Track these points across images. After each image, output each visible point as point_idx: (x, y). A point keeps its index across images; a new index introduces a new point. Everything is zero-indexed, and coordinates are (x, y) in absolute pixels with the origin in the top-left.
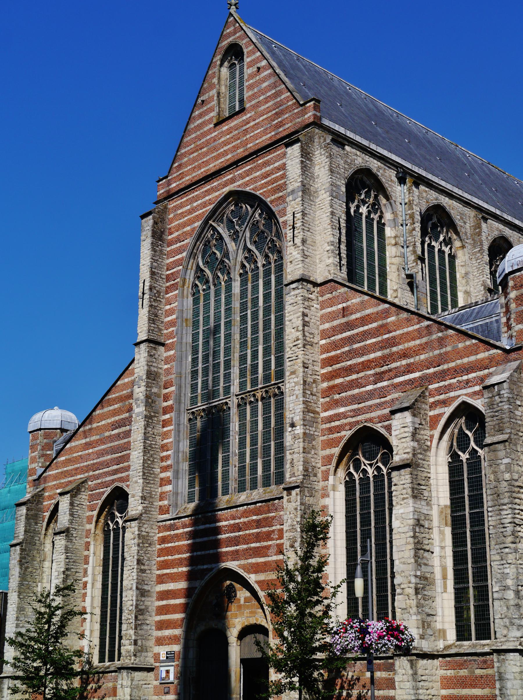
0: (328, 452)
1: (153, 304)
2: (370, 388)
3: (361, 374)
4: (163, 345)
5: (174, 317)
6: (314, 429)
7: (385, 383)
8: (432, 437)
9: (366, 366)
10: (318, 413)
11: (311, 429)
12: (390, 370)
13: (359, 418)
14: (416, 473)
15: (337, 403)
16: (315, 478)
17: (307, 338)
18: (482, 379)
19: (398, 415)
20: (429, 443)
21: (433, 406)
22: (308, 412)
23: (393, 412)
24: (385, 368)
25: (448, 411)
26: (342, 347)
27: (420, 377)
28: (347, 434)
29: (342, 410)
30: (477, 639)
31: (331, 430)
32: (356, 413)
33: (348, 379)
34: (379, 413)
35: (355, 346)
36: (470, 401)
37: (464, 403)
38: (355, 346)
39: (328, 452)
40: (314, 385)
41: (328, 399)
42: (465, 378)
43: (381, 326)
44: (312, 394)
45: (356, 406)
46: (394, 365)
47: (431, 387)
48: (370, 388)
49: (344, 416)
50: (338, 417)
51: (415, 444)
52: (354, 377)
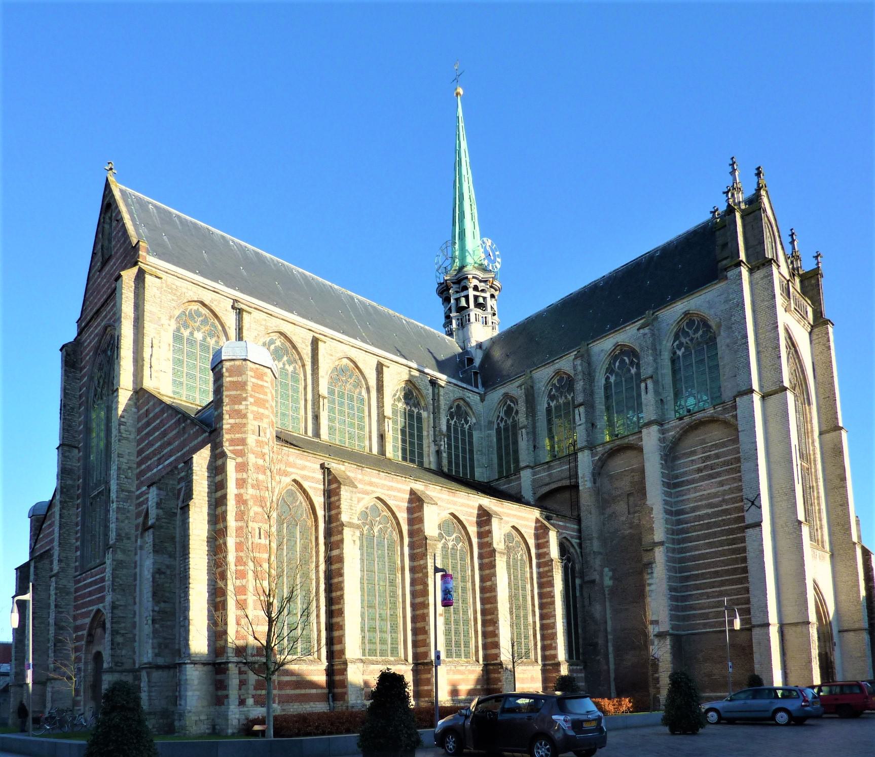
1: (67, 417)
2: (155, 470)
3: (152, 460)
6: (128, 504)
7: (160, 467)
8: (177, 506)
9: (154, 454)
10: (133, 492)
11: (125, 504)
12: (163, 456)
14: (158, 533)
16: (128, 541)
17: (123, 435)
20: (176, 511)
22: (123, 491)
24: (162, 454)
27: (175, 460)
33: (147, 465)
40: (129, 471)
41: (139, 481)
43: (161, 422)
44: (126, 477)
46: (165, 451)
48: (155, 470)
51: (160, 511)
52: (149, 463)
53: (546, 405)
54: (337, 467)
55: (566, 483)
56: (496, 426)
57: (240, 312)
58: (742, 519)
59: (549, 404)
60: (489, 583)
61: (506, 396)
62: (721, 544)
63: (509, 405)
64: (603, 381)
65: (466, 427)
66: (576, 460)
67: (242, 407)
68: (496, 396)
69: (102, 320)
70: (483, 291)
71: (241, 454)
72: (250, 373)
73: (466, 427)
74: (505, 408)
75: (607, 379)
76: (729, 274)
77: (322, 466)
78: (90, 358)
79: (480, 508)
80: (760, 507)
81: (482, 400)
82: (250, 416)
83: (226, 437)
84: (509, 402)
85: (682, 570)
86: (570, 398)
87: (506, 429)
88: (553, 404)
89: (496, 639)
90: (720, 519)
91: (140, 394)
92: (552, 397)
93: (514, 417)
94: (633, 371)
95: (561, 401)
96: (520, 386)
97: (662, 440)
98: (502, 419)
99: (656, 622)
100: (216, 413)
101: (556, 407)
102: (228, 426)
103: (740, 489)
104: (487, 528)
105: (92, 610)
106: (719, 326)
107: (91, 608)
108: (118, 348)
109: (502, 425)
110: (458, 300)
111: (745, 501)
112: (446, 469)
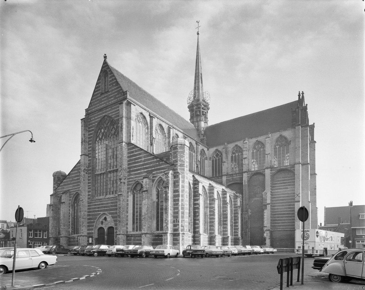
0: (128, 187)
4: (88, 156)
5: (91, 149)
8: (153, 185)
13: (136, 179)
15: (131, 175)
18: (165, 172)
19: (145, 179)
21: (153, 177)
23: (144, 178)
25: (157, 179)
26: (133, 161)
28: (133, 182)
29: (132, 177)
30: (160, 230)
31: (130, 181)
32: (136, 177)
34: (141, 178)
35: (136, 161)
36: (162, 176)
37: (160, 177)
38: (136, 161)
39: (128, 187)
42: (161, 171)
45: (135, 176)
47: (153, 173)
49: (133, 178)
50: (131, 178)
53: (231, 155)
54: (197, 177)
55: (239, 182)
56: (212, 159)
57: (151, 117)
58: (294, 199)
59: (232, 155)
60: (225, 213)
61: (217, 150)
62: (286, 205)
63: (218, 153)
64: (252, 151)
65: (203, 158)
66: (243, 175)
67: (183, 159)
68: (212, 150)
69: (104, 113)
70: (205, 109)
71: (183, 173)
72: (185, 149)
73: (203, 158)
74: (216, 154)
75: (253, 151)
76: (296, 127)
77: (193, 176)
78: (95, 125)
79: (223, 189)
80: (300, 197)
81: (208, 150)
82: (185, 162)
83: (179, 167)
84: (217, 152)
85: (273, 212)
86: (240, 154)
87: (216, 160)
88: (234, 155)
89: (227, 229)
90: (286, 198)
91: (129, 144)
92: (233, 153)
93: (219, 158)
94: (262, 150)
95: (237, 154)
96: (223, 148)
97: (271, 173)
98: (214, 157)
99: (266, 227)
100: (174, 159)
101: (234, 156)
102: (179, 164)
103: (294, 190)
104: (225, 196)
105: (100, 214)
106: (290, 141)
107: (100, 213)
108: (121, 128)
109: (214, 159)
110: (196, 112)
111: (295, 195)
112: (194, 171)
